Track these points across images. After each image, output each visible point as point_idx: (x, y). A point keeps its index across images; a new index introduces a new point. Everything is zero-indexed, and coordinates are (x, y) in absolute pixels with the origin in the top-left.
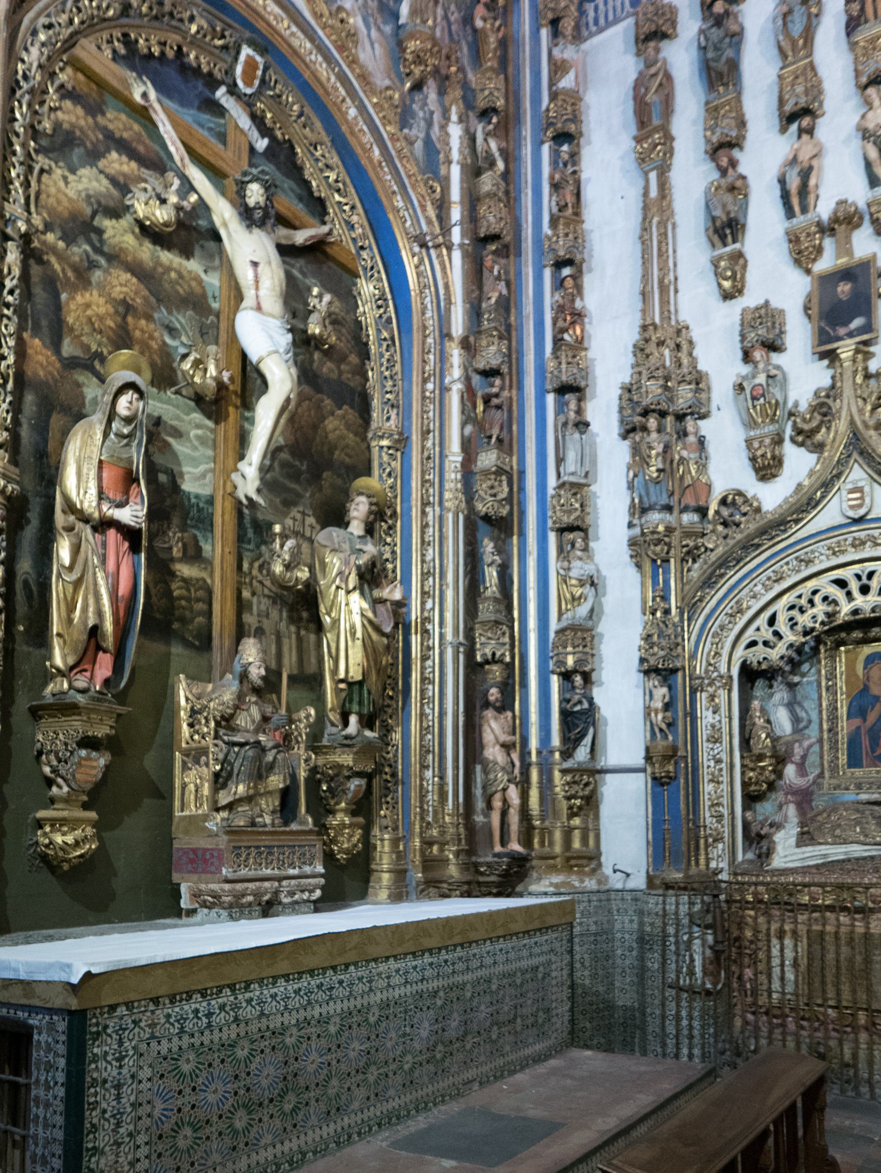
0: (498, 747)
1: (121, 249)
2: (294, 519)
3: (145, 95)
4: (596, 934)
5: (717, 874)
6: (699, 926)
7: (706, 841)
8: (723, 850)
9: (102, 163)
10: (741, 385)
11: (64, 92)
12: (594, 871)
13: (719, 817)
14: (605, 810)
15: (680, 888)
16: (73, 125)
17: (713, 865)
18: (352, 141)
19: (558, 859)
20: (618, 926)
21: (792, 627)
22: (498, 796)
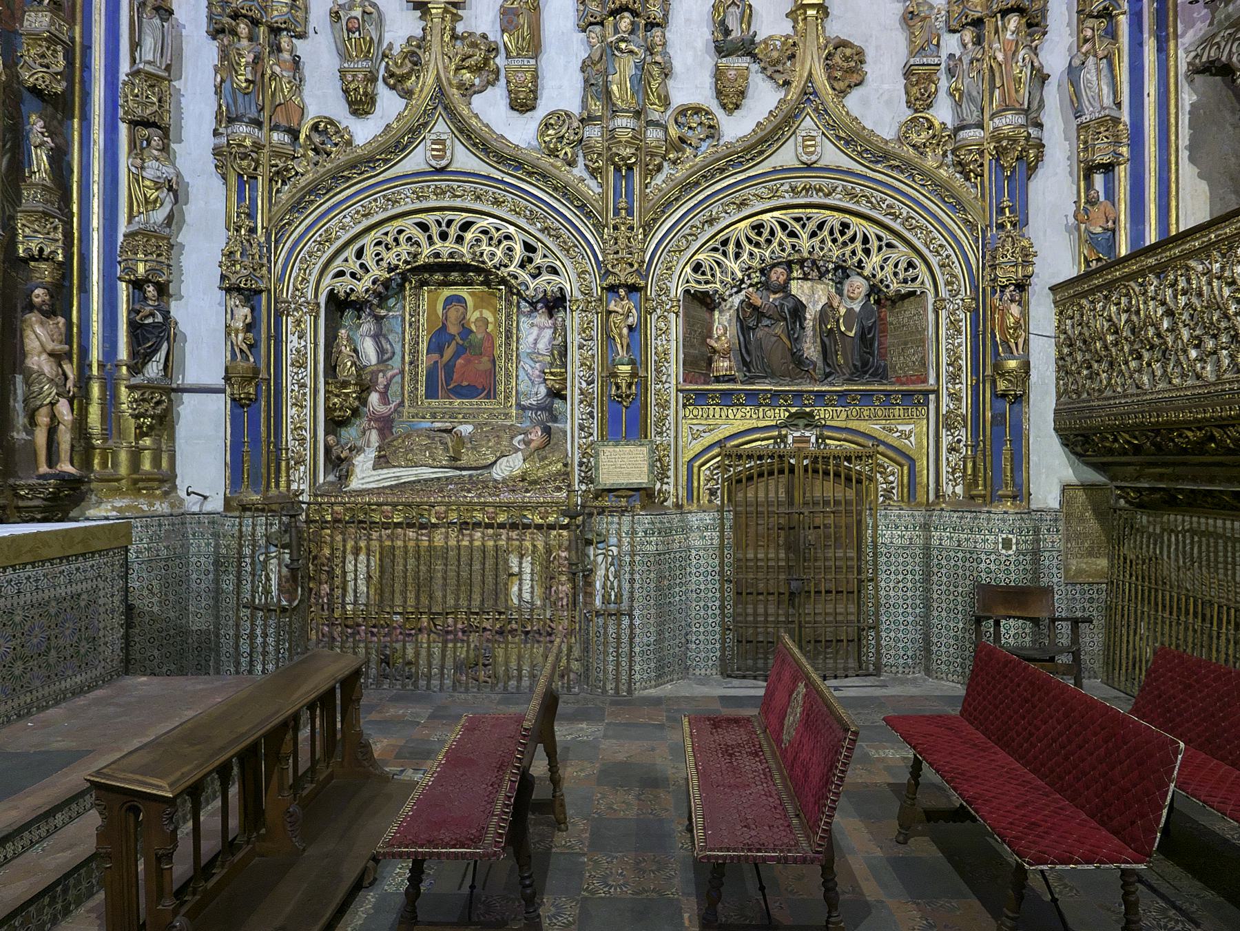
0: (44, 356)
4: (167, 560)
5: (298, 496)
6: (276, 546)
7: (288, 464)
8: (305, 472)
12: (166, 494)
14: (182, 431)
15: (257, 510)
17: (294, 486)
19: (124, 481)
20: (193, 550)
21: (377, 262)
22: (44, 411)
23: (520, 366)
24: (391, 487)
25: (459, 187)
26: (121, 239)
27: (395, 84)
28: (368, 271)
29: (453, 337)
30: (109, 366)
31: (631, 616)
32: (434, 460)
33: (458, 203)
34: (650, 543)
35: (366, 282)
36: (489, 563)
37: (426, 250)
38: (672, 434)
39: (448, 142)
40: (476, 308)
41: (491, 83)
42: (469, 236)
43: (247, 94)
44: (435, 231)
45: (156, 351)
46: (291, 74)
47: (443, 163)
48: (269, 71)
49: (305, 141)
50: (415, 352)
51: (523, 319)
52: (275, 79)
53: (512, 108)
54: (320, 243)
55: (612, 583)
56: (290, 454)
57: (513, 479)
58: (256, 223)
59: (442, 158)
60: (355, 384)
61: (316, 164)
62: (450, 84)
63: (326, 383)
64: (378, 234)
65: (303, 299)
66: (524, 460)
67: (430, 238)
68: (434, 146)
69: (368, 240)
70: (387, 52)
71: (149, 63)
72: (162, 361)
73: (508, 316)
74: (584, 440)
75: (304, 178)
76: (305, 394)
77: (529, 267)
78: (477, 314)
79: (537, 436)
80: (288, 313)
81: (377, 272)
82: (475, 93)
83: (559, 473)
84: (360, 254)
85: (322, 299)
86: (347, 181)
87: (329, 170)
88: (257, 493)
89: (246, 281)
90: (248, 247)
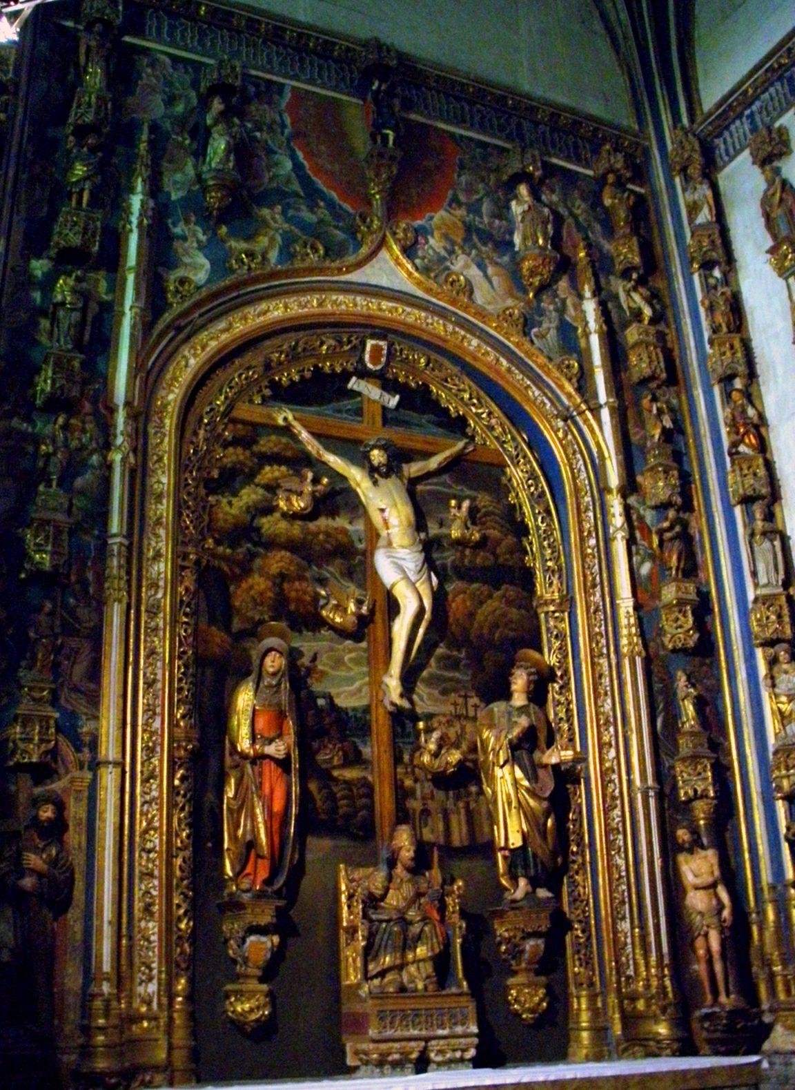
1: (276, 535)
2: (455, 704)
3: (285, 419)
9: (256, 480)
11: (226, 445)
16: (234, 463)
18: (477, 365)
26: (771, 757)
30: (779, 888)
71: (765, 586)
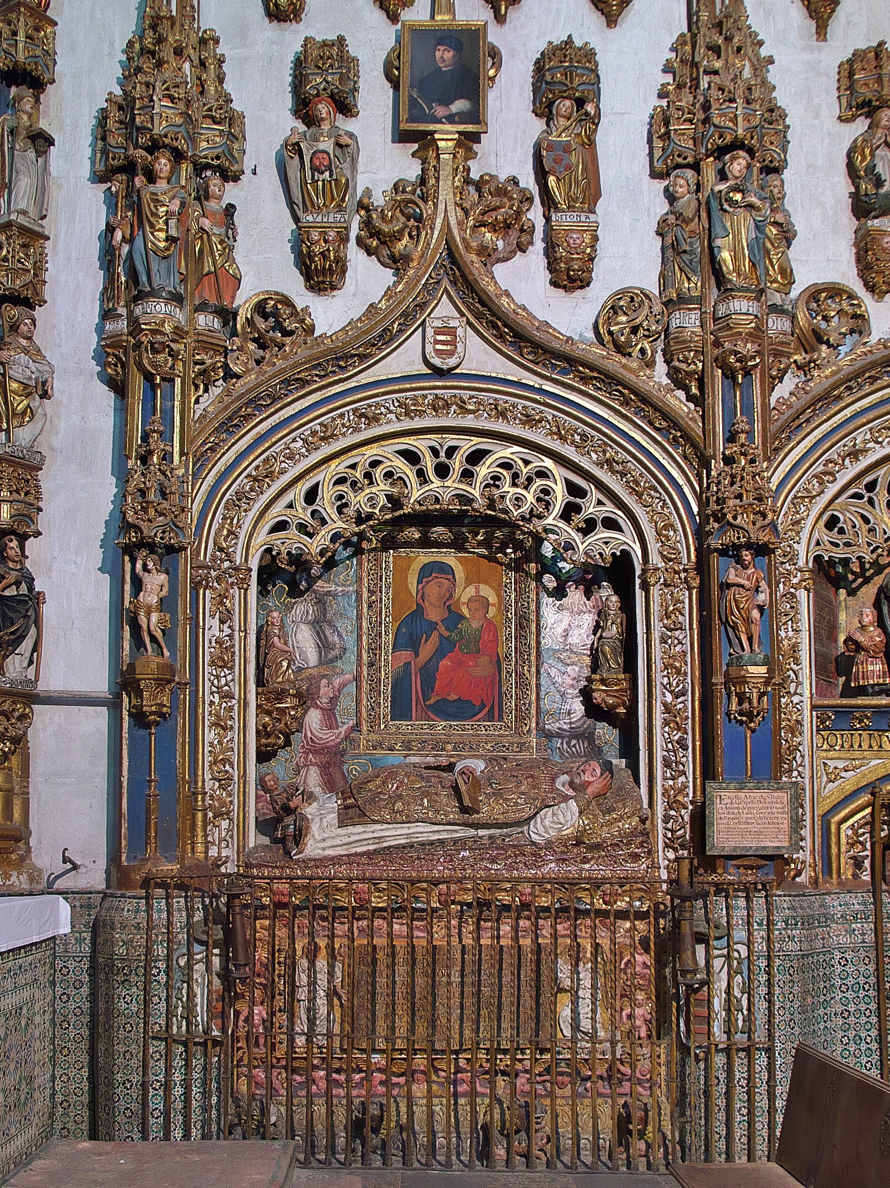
10: (297, 144)
13: (224, 781)
21: (340, 510)
23: (542, 670)
24: (367, 853)
25: (472, 397)
27: (377, 248)
28: (324, 522)
29: (433, 626)
31: (770, 1051)
32: (437, 812)
33: (469, 421)
34: (791, 938)
35: (322, 539)
36: (527, 973)
37: (416, 493)
38: (807, 774)
39: (460, 332)
40: (468, 582)
41: (522, 248)
42: (483, 471)
43: (165, 258)
44: (429, 463)
45: (22, 638)
46: (223, 230)
47: (452, 362)
48: (194, 227)
49: (243, 327)
50: (375, 649)
51: (546, 600)
52: (201, 238)
53: (554, 284)
54: (255, 479)
55: (739, 1001)
56: (208, 801)
57: (563, 841)
58: (172, 446)
59: (451, 353)
60: (294, 696)
61: (258, 362)
62: (467, 247)
63: (257, 694)
64: (341, 468)
65: (227, 564)
66: (581, 813)
67: (421, 474)
68: (439, 338)
69: (325, 476)
70: (366, 201)
72: (28, 654)
73: (520, 593)
74: (671, 782)
75: (241, 382)
76: (231, 709)
77: (578, 519)
78: (471, 591)
79: (593, 775)
80: (208, 583)
81: (340, 524)
82: (499, 260)
83: (633, 833)
84: (311, 496)
85: (254, 564)
86: (303, 387)
87: (283, 371)
88: (170, 860)
89: (164, 532)
90: (166, 483)
